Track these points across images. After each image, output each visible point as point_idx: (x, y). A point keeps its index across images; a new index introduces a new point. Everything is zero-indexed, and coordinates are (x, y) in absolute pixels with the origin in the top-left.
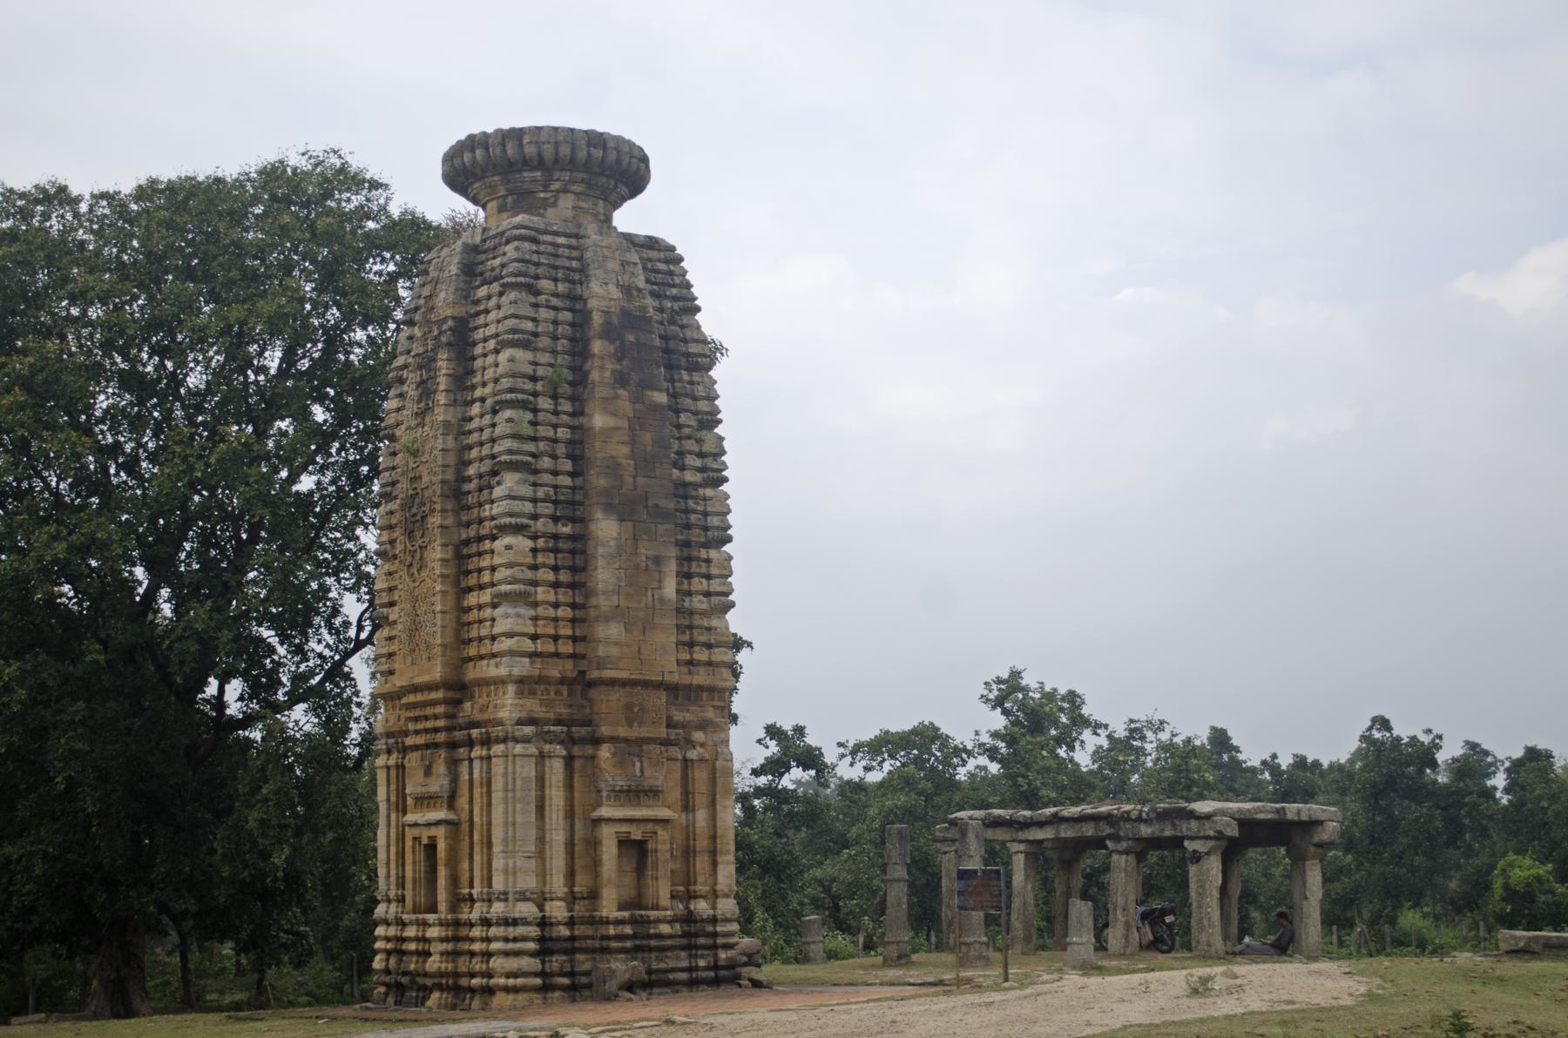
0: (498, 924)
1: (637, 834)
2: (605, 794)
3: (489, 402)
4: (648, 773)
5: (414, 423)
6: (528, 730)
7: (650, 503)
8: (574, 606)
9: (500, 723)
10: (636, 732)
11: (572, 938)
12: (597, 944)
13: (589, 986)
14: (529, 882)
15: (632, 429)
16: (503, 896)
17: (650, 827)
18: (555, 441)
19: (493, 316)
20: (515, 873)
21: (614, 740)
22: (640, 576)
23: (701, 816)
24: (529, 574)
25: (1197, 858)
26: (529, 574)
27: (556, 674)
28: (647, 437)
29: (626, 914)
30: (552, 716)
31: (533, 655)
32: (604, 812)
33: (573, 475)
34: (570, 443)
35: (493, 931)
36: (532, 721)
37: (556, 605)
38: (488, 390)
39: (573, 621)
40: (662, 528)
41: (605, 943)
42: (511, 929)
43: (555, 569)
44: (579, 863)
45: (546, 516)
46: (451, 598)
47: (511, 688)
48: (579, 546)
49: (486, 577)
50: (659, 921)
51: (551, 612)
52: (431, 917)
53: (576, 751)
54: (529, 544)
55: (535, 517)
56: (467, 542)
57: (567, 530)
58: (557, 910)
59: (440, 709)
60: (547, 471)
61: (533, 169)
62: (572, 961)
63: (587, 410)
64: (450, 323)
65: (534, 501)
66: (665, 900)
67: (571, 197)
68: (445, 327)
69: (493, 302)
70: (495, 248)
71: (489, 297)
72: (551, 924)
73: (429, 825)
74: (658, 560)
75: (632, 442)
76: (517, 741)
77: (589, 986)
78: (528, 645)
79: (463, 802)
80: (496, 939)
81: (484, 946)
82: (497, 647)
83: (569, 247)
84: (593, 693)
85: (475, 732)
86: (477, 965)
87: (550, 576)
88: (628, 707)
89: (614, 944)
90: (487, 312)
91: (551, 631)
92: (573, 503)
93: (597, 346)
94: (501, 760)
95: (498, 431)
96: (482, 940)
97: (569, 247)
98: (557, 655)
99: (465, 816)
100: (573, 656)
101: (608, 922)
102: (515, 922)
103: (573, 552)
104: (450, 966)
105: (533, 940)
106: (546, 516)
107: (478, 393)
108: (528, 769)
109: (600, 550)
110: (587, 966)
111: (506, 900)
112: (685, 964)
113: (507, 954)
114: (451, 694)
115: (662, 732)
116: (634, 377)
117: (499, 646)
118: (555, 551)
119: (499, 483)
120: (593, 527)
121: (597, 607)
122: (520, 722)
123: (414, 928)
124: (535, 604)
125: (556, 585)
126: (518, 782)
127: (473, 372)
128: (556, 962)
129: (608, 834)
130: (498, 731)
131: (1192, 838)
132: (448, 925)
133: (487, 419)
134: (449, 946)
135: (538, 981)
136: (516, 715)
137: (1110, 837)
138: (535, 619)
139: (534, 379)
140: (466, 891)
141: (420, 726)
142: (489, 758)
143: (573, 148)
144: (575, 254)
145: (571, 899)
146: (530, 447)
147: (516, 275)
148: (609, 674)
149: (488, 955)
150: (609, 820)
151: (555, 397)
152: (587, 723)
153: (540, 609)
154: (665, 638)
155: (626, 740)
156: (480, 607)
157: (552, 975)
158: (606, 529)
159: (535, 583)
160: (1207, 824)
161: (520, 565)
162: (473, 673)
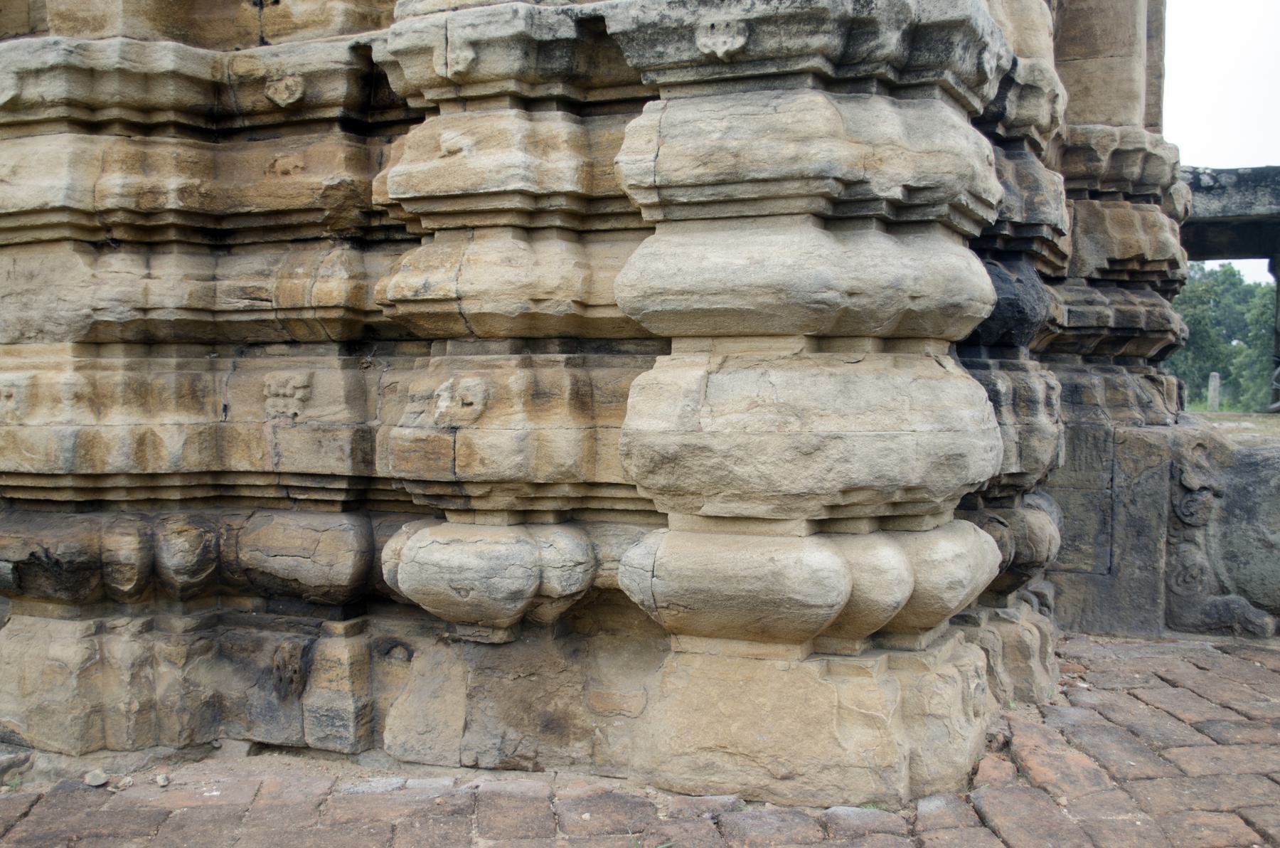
12: (1107, 308)
35: (658, 142)
42: (883, 117)
80: (682, 205)
81: (547, 271)
86: (507, 424)
96: (532, 217)
113: (832, 329)
132: (143, 125)
149: (594, 343)
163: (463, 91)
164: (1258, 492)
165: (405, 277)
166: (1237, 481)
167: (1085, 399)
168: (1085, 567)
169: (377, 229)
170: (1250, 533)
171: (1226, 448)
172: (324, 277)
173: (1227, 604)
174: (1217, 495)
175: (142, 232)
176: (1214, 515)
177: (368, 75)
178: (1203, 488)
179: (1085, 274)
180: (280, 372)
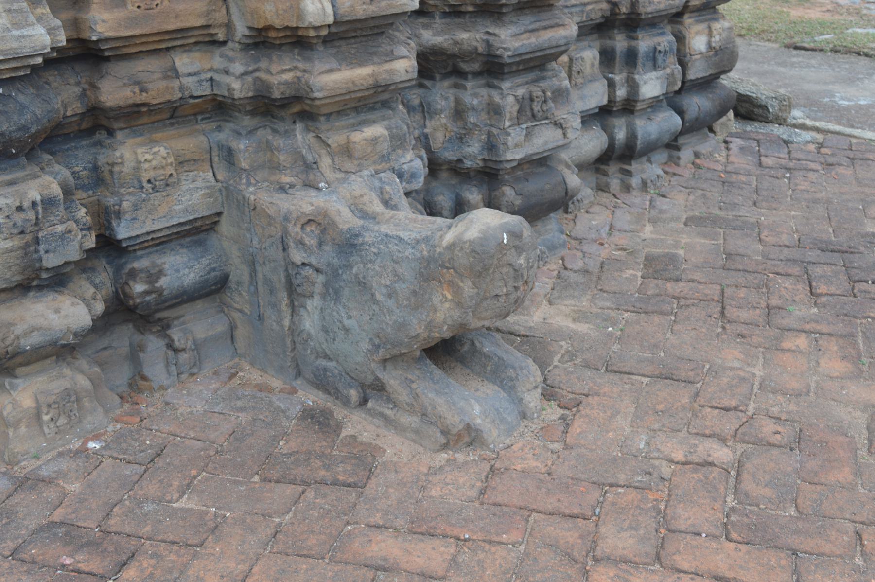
12: (236, 77)
41: (281, 73)
89: (331, 77)
110: (191, 198)
164: (344, 276)
166: (336, 261)
167: (236, 162)
168: (246, 310)
170: (335, 313)
171: (338, 227)
173: (325, 370)
174: (318, 271)
176: (318, 289)
178: (304, 264)
179: (237, 39)
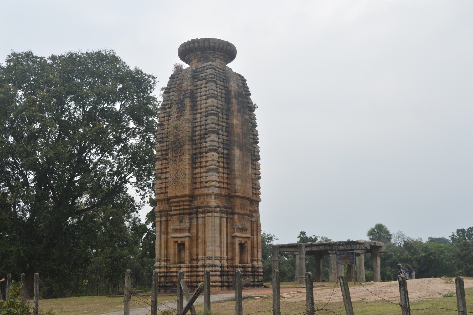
0: (209, 267)
1: (243, 242)
2: (236, 229)
3: (204, 114)
4: (245, 223)
5: (176, 119)
6: (218, 209)
7: (246, 146)
8: (227, 174)
9: (209, 207)
10: (243, 212)
11: (228, 272)
13: (232, 286)
14: (218, 254)
15: (242, 125)
16: (210, 259)
17: (246, 239)
18: (223, 126)
19: (204, 89)
20: (215, 251)
21: (238, 213)
22: (244, 166)
23: (255, 237)
24: (217, 164)
25: (358, 255)
26: (217, 164)
27: (224, 193)
28: (245, 128)
29: (240, 265)
30: (223, 205)
31: (219, 187)
32: (237, 234)
33: (227, 136)
34: (226, 127)
36: (218, 207)
37: (223, 173)
38: (204, 110)
39: (227, 178)
40: (249, 154)
42: (214, 268)
43: (223, 163)
44: (229, 249)
45: (221, 147)
46: (190, 170)
47: (213, 197)
48: (229, 157)
49: (204, 164)
50: (248, 267)
51: (222, 175)
52: (182, 265)
53: (229, 216)
54: (217, 155)
55: (219, 147)
56: (195, 154)
57: (226, 152)
58: (225, 263)
59: (187, 203)
60: (221, 134)
61: (211, 50)
62: (228, 278)
63: (230, 118)
64: (189, 91)
65: (219, 143)
66: (249, 262)
67: (219, 60)
68: (187, 92)
69: (203, 85)
70: (202, 71)
71: (201, 85)
72: (223, 267)
73: (182, 237)
74: (248, 163)
75: (242, 129)
76: (215, 212)
77: (232, 286)
78: (217, 184)
79: (194, 231)
82: (208, 184)
83: (222, 73)
84: (232, 200)
85: (200, 210)
87: (222, 165)
88: (241, 204)
90: (201, 88)
91: (223, 181)
92: (227, 145)
93: (234, 100)
94: (211, 218)
95: (208, 122)
97: (222, 73)
98: (223, 188)
99: (195, 234)
100: (227, 189)
101: (237, 267)
102: (215, 266)
103: (227, 158)
104: (190, 280)
105: (219, 272)
106: (221, 147)
107: (199, 111)
108: (217, 220)
109: (236, 158)
111: (212, 259)
112: (252, 280)
114: (190, 199)
115: (249, 213)
116: (242, 111)
117: (208, 184)
118: (223, 158)
119: (209, 137)
120: (233, 151)
121: (235, 174)
122: (215, 207)
123: (175, 269)
124: (218, 173)
125: (223, 167)
126: (216, 224)
127: (196, 106)
128: (225, 278)
129: (237, 241)
130: (210, 209)
131: (357, 250)
132: (189, 267)
133: (204, 118)
134: (189, 274)
135: (220, 284)
136: (215, 205)
137: (329, 250)
138: (219, 177)
139: (218, 108)
140: (196, 257)
141: (177, 208)
142: (205, 217)
143: (223, 45)
144: (224, 75)
145: (228, 260)
146: (217, 127)
147: (212, 78)
148: (238, 194)
150: (238, 237)
151: (222, 114)
152: (230, 208)
153: (220, 174)
154: (249, 185)
155: (240, 214)
156: (201, 173)
157: (224, 282)
158: (237, 152)
159: (219, 166)
160: (362, 246)
161: (216, 161)
162: (197, 192)
163: (200, 267)
165: (198, 274)
169: (198, 272)
172: (195, 274)
175: (188, 272)
177: (197, 266)
180: (194, 277)
